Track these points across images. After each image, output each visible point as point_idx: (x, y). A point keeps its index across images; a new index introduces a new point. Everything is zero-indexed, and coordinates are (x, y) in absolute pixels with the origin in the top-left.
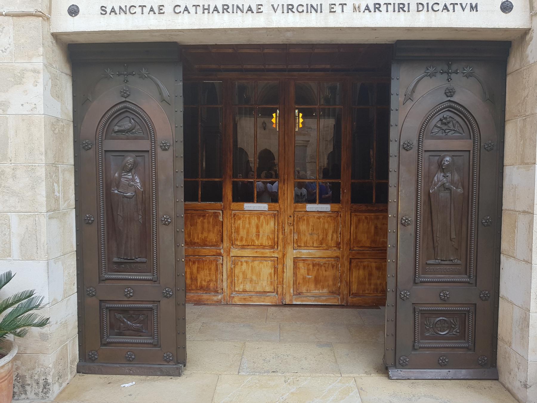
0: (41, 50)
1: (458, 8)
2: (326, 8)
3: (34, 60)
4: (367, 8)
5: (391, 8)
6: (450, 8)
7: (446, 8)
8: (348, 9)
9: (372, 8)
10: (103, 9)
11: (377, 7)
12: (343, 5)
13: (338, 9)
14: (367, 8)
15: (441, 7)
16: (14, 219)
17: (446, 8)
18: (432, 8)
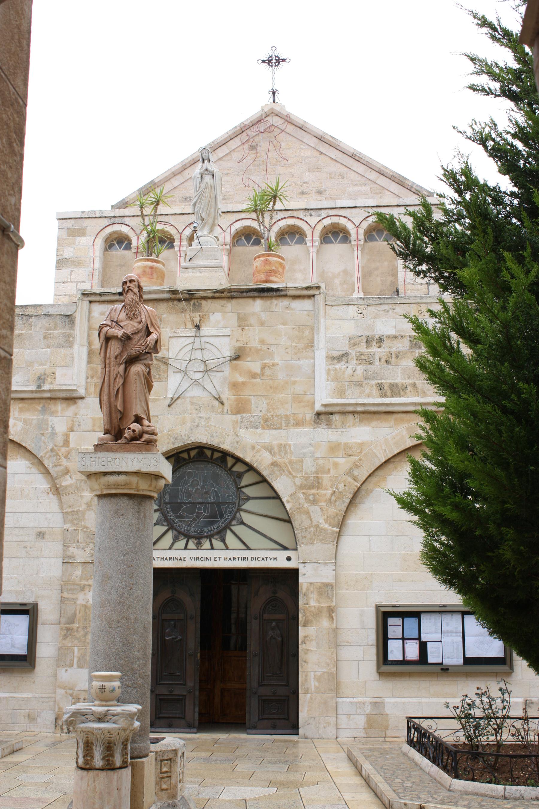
1: (268, 559)
2: (213, 559)
3: (89, 581)
4: (230, 559)
5: (240, 559)
6: (265, 559)
7: (263, 559)
8: (222, 559)
9: (232, 559)
11: (234, 559)
12: (220, 558)
13: (218, 559)
14: (230, 559)
15: (261, 559)
16: (76, 650)
17: (263, 559)
18: (258, 559)
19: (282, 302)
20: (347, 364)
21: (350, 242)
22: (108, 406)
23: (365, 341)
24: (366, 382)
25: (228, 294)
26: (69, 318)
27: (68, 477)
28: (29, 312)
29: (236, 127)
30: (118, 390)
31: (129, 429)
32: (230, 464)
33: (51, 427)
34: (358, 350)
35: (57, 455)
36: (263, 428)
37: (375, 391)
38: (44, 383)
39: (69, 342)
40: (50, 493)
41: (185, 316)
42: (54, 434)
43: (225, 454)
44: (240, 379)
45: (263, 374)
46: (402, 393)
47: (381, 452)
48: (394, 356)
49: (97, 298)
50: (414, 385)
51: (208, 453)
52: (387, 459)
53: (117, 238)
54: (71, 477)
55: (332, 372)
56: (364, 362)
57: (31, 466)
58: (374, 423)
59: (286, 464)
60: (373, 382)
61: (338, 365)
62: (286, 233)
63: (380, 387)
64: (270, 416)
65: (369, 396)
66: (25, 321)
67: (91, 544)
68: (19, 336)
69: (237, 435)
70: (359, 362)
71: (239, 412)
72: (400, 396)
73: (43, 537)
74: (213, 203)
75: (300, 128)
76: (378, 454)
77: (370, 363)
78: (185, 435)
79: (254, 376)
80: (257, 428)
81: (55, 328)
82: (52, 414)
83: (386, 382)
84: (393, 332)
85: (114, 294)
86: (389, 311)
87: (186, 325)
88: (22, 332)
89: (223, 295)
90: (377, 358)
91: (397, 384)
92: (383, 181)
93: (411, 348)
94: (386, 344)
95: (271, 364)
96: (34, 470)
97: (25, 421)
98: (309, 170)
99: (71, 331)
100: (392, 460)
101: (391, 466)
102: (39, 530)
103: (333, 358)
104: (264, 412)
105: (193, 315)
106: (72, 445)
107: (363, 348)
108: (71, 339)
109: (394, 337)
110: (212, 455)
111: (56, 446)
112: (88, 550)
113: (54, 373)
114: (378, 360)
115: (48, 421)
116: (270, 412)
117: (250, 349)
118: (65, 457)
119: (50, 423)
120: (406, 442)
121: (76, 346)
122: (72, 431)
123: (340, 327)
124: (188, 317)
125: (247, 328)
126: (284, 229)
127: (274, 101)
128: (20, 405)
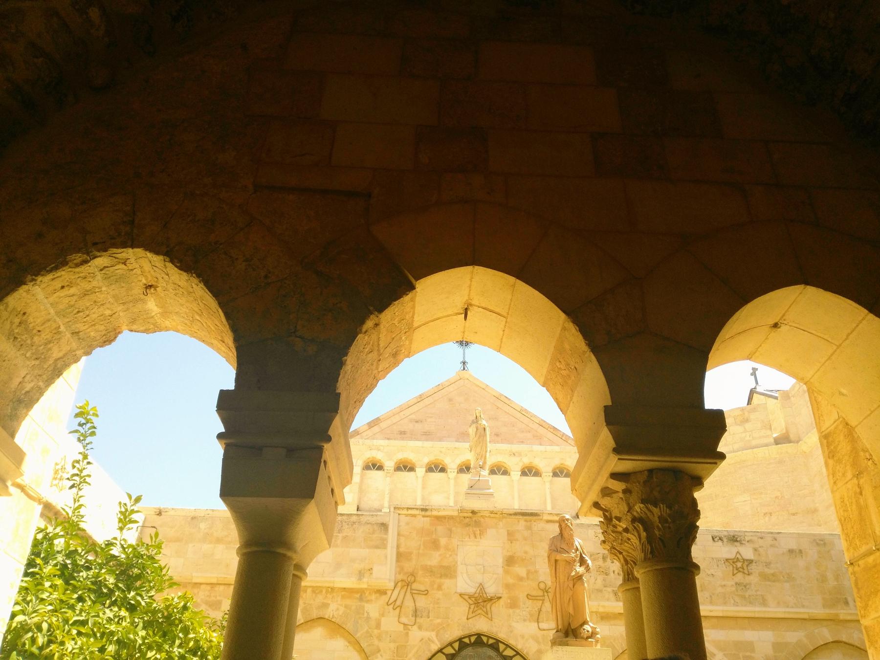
20: (590, 574)
21: (541, 476)
22: (560, 610)
23: (601, 557)
24: (605, 589)
25: (501, 516)
26: (384, 526)
27: (379, 655)
29: (439, 385)
30: (570, 599)
31: (584, 629)
32: (501, 650)
33: (367, 612)
34: (597, 563)
35: (371, 636)
36: (530, 621)
38: (364, 576)
39: (382, 545)
41: (469, 529)
42: (368, 618)
43: (498, 641)
44: (511, 581)
45: (528, 578)
49: (405, 512)
51: (485, 639)
53: (371, 461)
54: (381, 655)
57: (348, 644)
60: (610, 589)
62: (495, 466)
64: (535, 612)
65: (608, 600)
66: (350, 526)
68: (345, 537)
69: (511, 626)
74: (485, 448)
76: (616, 646)
77: (607, 574)
78: (471, 624)
79: (521, 579)
80: (525, 620)
81: (373, 533)
82: (368, 601)
85: (417, 509)
88: (346, 534)
90: (611, 571)
92: (541, 431)
96: (351, 648)
97: (346, 606)
98: (490, 419)
99: (385, 536)
105: (475, 529)
106: (383, 628)
110: (488, 642)
111: (370, 628)
114: (612, 573)
115: (364, 608)
117: (518, 558)
118: (377, 637)
119: (366, 609)
121: (389, 548)
122: (383, 616)
124: (471, 530)
125: (514, 542)
127: (464, 369)
128: (343, 593)
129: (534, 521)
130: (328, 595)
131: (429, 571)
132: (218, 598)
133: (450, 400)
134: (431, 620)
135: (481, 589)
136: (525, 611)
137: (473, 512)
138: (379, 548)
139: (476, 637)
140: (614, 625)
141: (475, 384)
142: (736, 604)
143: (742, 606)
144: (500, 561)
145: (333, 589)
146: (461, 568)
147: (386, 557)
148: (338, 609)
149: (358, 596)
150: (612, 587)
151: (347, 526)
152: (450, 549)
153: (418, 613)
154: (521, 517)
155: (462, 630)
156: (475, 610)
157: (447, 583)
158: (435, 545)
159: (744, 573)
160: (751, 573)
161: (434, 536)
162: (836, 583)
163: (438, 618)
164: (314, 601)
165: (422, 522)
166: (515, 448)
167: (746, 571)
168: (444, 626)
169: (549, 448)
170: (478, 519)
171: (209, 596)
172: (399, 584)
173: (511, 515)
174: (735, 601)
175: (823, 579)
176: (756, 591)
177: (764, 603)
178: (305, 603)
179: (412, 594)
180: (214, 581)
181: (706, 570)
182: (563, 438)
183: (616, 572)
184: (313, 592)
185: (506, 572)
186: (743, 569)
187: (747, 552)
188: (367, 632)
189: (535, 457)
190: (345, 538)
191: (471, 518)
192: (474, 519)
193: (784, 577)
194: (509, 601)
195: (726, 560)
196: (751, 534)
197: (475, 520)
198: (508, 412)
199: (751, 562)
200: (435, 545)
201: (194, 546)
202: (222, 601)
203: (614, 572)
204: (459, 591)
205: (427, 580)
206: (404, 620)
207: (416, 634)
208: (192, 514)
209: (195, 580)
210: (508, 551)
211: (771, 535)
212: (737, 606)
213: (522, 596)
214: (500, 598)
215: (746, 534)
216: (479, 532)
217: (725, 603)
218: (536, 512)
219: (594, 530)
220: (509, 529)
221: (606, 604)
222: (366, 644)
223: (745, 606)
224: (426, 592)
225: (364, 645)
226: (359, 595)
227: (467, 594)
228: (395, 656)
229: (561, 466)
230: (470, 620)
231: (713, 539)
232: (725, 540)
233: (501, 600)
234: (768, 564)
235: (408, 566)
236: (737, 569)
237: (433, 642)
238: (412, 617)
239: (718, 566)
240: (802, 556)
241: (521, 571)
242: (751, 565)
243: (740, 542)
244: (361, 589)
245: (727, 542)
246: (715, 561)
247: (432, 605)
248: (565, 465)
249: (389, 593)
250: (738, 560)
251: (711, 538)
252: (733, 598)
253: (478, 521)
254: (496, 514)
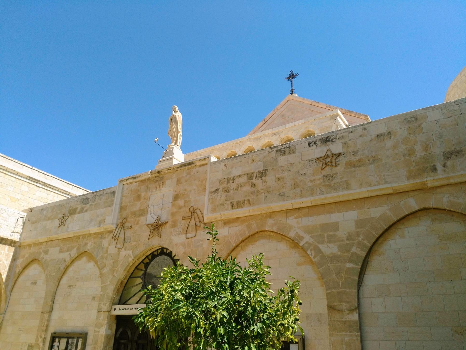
0: (107, 319)
10: (119, 309)
19: (195, 169)
20: (218, 194)
24: (226, 202)
26: (114, 193)
28: (101, 192)
36: (182, 234)
37: (230, 206)
40: (100, 278)
41: (157, 183)
42: (103, 248)
44: (175, 210)
45: (184, 206)
46: (242, 205)
47: (233, 240)
48: (239, 186)
50: (249, 200)
52: (236, 245)
54: (106, 269)
55: (211, 200)
56: (225, 192)
58: (231, 225)
59: (189, 252)
60: (229, 202)
61: (214, 195)
63: (232, 204)
65: (227, 210)
67: (108, 302)
69: (171, 239)
70: (223, 192)
71: (173, 227)
72: (241, 207)
73: (94, 300)
75: (302, 102)
76: (231, 242)
77: (228, 192)
79: (180, 208)
80: (179, 234)
82: (104, 238)
83: (235, 201)
84: (239, 174)
86: (238, 163)
87: (157, 188)
88: (97, 202)
89: (171, 171)
91: (240, 201)
93: (248, 180)
94: (236, 181)
95: (188, 201)
97: (95, 243)
99: (113, 199)
100: (241, 245)
101: (239, 248)
102: (93, 296)
103: (212, 192)
104: (183, 226)
105: (160, 183)
107: (225, 185)
108: (113, 202)
109: (240, 176)
112: (107, 305)
113: (105, 219)
116: (186, 225)
117: (180, 194)
120: (246, 233)
123: (216, 176)
125: (180, 184)
126: (265, 144)
128: (94, 236)
129: (193, 168)
130: (89, 239)
131: (134, 214)
132: (48, 248)
133: (283, 116)
134: (131, 243)
135: (158, 219)
136: (180, 228)
137: (159, 172)
138: (110, 206)
139: (161, 250)
140: (232, 227)
141: (297, 101)
142: (322, 193)
143: (327, 194)
144: (171, 199)
145: (90, 234)
146: (151, 208)
147: (112, 211)
148: (91, 245)
149: (100, 236)
150: (231, 200)
151: (97, 198)
152: (146, 198)
153: (126, 240)
154: (184, 168)
155: (145, 247)
156: (153, 232)
157: (142, 219)
158: (139, 197)
159: (332, 166)
160: (338, 165)
161: (139, 193)
162: (424, 153)
163: (134, 242)
164: (82, 242)
165: (135, 186)
166: (275, 130)
167: (334, 164)
168: (137, 246)
169: (296, 123)
170: (162, 176)
171: (45, 248)
172: (119, 225)
173: (178, 168)
174: (321, 191)
175: (411, 152)
176: (341, 178)
177: (347, 186)
178: (78, 245)
179: (124, 230)
180: (46, 240)
181: (300, 171)
182: (357, 116)
183: (234, 189)
184: (83, 238)
185: (173, 205)
186: (332, 163)
187: (336, 148)
188: (102, 255)
189: (288, 132)
190: (96, 204)
191: (159, 176)
192: (160, 177)
193: (369, 161)
194: (172, 223)
195: (318, 159)
196: (342, 131)
197: (161, 177)
198: (318, 111)
199: (339, 154)
200: (139, 197)
201: (41, 223)
202: (49, 249)
203: (233, 189)
204: (147, 223)
205: (132, 220)
206: (119, 246)
207: (123, 253)
208: (42, 208)
209: (40, 241)
210: (176, 191)
211: (361, 127)
212: (323, 194)
213: (179, 218)
214: (167, 222)
215: (338, 132)
216: (161, 184)
217: (312, 194)
218: (191, 161)
219: (224, 163)
220: (178, 177)
221: (226, 213)
222: (100, 263)
223: (330, 192)
224: (131, 227)
225: (99, 263)
226: (101, 235)
227: (151, 224)
228: (112, 268)
229: (310, 132)
230: (150, 240)
231: (309, 145)
232: (319, 143)
233: (168, 225)
234: (355, 153)
235: (124, 214)
236: (326, 164)
237: (130, 256)
238: (123, 243)
239: (310, 166)
240: (390, 137)
241: (181, 202)
242: (339, 158)
243: (332, 141)
244: (102, 231)
245: (320, 144)
246: (308, 162)
247: (132, 234)
248: (311, 131)
249: (114, 231)
250: (328, 156)
251: (307, 145)
252: (319, 189)
253: (162, 177)
254: (171, 169)
